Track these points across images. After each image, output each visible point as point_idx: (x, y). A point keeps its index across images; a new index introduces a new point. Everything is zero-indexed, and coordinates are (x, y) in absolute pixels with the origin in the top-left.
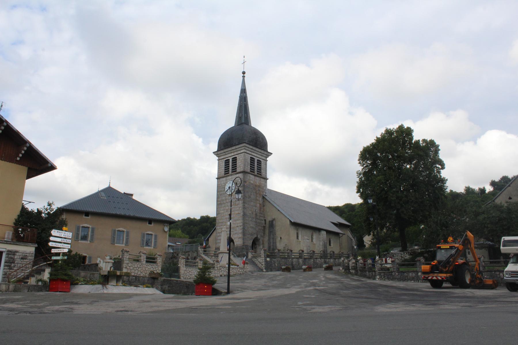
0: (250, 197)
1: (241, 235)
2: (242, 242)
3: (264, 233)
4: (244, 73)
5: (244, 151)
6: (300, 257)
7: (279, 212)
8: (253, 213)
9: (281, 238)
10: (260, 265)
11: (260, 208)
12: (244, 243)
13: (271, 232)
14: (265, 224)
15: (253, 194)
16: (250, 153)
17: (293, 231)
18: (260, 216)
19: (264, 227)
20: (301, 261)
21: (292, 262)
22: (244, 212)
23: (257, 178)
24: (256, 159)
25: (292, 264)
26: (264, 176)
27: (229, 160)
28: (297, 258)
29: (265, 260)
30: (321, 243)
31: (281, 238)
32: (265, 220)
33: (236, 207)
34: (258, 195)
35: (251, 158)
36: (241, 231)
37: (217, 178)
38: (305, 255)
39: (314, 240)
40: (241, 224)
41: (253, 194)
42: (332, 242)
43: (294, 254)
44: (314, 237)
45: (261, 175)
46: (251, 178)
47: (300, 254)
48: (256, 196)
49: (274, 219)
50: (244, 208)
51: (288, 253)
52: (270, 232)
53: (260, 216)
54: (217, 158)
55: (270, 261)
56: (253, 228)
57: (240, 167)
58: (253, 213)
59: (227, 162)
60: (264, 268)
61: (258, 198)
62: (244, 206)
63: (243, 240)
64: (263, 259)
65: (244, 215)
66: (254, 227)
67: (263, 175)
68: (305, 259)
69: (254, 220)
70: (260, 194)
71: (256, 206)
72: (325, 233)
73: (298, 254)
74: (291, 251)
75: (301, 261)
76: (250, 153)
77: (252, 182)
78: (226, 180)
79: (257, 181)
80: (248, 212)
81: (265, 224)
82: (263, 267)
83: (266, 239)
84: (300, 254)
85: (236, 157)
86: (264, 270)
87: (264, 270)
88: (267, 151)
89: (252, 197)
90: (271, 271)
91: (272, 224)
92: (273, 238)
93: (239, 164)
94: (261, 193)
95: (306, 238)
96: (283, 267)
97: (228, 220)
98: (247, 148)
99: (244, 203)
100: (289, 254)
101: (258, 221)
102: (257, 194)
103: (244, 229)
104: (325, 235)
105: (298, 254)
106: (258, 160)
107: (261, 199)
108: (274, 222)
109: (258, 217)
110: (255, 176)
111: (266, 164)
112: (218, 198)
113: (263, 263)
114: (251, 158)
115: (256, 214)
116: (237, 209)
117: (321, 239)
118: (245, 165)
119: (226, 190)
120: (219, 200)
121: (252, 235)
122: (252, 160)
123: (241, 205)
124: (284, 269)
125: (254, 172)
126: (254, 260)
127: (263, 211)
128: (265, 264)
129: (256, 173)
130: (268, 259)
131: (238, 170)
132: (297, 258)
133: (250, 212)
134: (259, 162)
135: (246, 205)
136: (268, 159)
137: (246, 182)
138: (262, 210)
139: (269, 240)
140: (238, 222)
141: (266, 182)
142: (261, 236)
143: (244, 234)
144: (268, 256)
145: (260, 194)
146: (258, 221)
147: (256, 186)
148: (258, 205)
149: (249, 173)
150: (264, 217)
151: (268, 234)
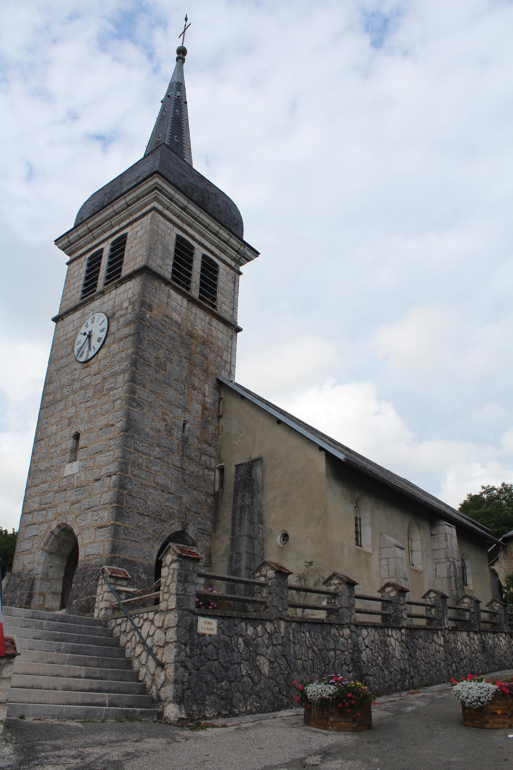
0: (161, 366)
1: (106, 516)
2: (107, 546)
3: (215, 522)
4: (182, 52)
5: (155, 204)
6: (389, 621)
7: (278, 430)
8: (169, 432)
9: (285, 537)
10: (145, 668)
11: (205, 423)
12: (114, 549)
13: (242, 509)
14: (222, 482)
15: (175, 358)
16: (179, 222)
17: (337, 503)
18: (203, 453)
19: (217, 496)
20: (394, 638)
21: (356, 649)
22: (128, 416)
23: (201, 314)
24: (199, 252)
25: (356, 663)
26: (228, 318)
27: (102, 251)
28: (375, 626)
29: (187, 629)
30: (443, 570)
31: (285, 537)
32: (222, 470)
33: (104, 399)
34: (197, 371)
35: (178, 237)
36: (108, 497)
37: (56, 320)
38: (416, 614)
39: (417, 557)
40: (113, 468)
41: (175, 358)
42: (468, 570)
43: (359, 604)
44: (417, 544)
45: (214, 307)
46: (175, 305)
47: (386, 602)
48: (191, 373)
49: (259, 460)
50: (132, 399)
51: (334, 595)
52: (239, 510)
53: (203, 453)
54: (68, 259)
55: (224, 643)
56: (165, 489)
57: (133, 259)
58: (169, 432)
59: (94, 263)
60: (168, 692)
61: (197, 383)
62: (132, 392)
63: (115, 534)
64: (172, 619)
65: (130, 428)
66: (173, 488)
67: (223, 309)
68: (412, 630)
69: (175, 459)
70: (206, 371)
71: (185, 410)
72: (452, 531)
73: (377, 606)
74: (351, 584)
75: (394, 638)
76: (179, 222)
77: (175, 316)
78: (84, 316)
79: (200, 321)
80: (150, 423)
81: (222, 482)
82: (163, 682)
83: (223, 543)
84: (386, 602)
85: (125, 235)
86: (172, 711)
87: (172, 711)
88: (240, 237)
89: (174, 368)
90: (228, 710)
91: (248, 478)
92: (251, 538)
93: (134, 250)
94: (212, 368)
95: (394, 541)
96: (316, 690)
97: (68, 456)
98: (167, 201)
99: (133, 380)
100: (341, 602)
101: (193, 468)
102: (193, 364)
103: (121, 486)
104: (455, 540)
105: (377, 606)
106: (204, 257)
107: (208, 388)
108: (258, 471)
109: (194, 454)
110: (191, 300)
111: (235, 283)
112: (48, 382)
113: (169, 655)
114: (178, 237)
115: (185, 440)
116: (106, 407)
117: (442, 554)
118: (151, 249)
119: (77, 348)
120: (51, 388)
121: (158, 518)
122: (183, 251)
123: (121, 391)
124: (324, 702)
125: (188, 289)
126: (120, 626)
127: (216, 436)
128: (180, 664)
129: (195, 293)
130: (207, 626)
131: (126, 270)
132: (375, 626)
133: (160, 425)
134: (210, 269)
135: (142, 393)
136: (242, 269)
137: (150, 308)
138: (211, 428)
139: (234, 542)
140: (101, 459)
141: (233, 339)
142: (203, 531)
143: (120, 508)
144: (206, 604)
145: (206, 371)
146: (193, 468)
147: (192, 336)
148: (198, 407)
149: (166, 282)
150: (219, 459)
151: (229, 526)
